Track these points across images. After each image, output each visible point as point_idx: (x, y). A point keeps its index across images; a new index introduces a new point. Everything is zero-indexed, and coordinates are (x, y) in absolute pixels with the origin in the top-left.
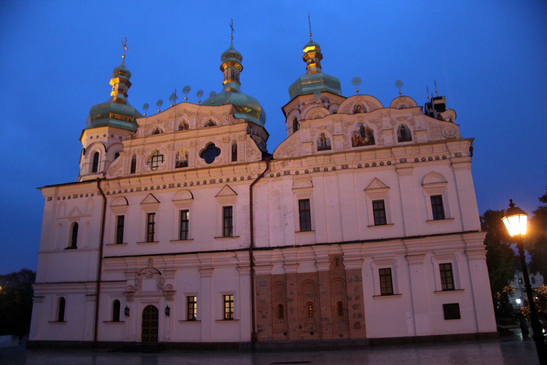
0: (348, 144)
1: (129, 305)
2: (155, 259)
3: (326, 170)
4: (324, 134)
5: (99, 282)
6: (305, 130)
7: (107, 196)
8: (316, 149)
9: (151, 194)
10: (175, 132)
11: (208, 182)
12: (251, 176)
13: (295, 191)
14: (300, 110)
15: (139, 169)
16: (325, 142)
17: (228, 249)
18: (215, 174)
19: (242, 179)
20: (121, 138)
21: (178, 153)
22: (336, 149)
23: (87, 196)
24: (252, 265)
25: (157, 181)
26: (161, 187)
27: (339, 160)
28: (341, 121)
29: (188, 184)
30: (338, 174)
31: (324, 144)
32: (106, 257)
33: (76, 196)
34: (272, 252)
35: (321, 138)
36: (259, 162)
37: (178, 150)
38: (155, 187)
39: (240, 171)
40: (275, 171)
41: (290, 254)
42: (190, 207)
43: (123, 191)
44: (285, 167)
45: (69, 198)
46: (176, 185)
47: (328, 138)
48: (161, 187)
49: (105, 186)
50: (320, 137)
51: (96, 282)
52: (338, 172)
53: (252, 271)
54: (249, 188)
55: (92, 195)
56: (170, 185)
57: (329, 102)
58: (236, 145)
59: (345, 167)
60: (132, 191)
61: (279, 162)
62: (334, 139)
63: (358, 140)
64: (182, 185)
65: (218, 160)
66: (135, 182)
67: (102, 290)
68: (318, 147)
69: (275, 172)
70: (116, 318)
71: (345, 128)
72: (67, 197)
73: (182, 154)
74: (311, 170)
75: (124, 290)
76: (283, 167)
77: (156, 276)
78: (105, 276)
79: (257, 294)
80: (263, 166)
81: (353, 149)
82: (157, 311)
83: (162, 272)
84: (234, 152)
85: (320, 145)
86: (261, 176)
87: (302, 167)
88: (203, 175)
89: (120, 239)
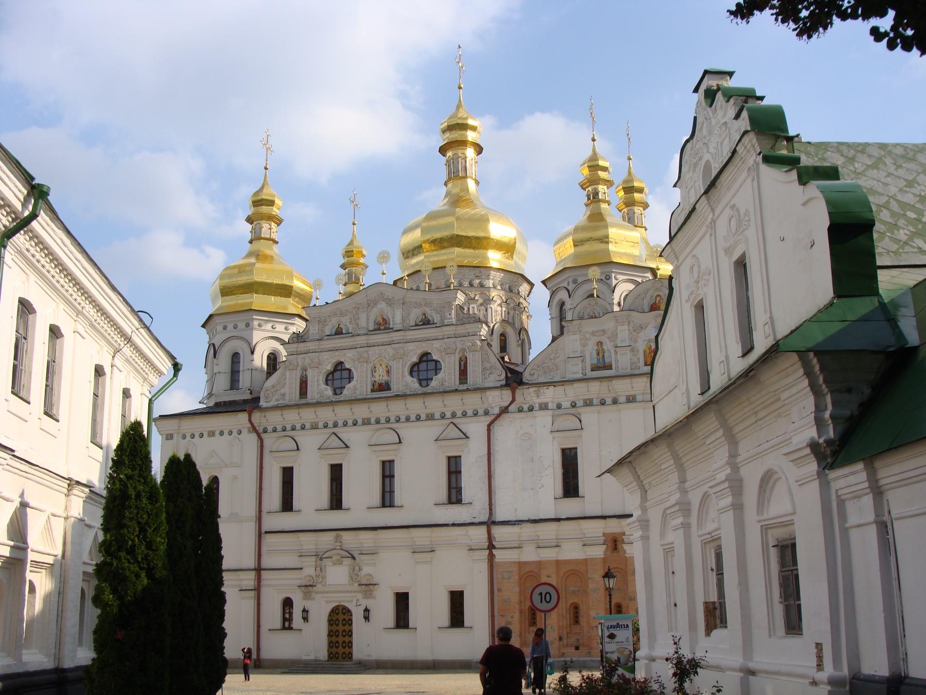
0: (638, 361)
1: (309, 605)
2: (346, 536)
3: (603, 403)
4: (601, 343)
5: (259, 570)
6: (572, 337)
7: (263, 436)
8: (589, 368)
9: (334, 433)
10: (369, 333)
12: (489, 409)
16: (604, 356)
17: (456, 522)
18: (435, 405)
19: (476, 414)
20: (274, 327)
21: (375, 367)
22: (620, 371)
23: (230, 433)
24: (491, 547)
25: (343, 413)
26: (350, 422)
27: (622, 388)
30: (620, 411)
31: (601, 360)
32: (266, 532)
33: (212, 434)
34: (521, 528)
35: (597, 350)
37: (375, 362)
38: (340, 423)
39: (472, 401)
41: (548, 532)
45: (201, 436)
46: (373, 421)
47: (608, 350)
50: (596, 348)
51: (255, 569)
52: (620, 406)
53: (491, 557)
54: (486, 428)
55: (240, 432)
56: (363, 420)
58: (466, 358)
59: (631, 400)
61: (532, 390)
62: (616, 353)
64: (383, 420)
65: (437, 382)
66: (308, 415)
67: (263, 583)
68: (591, 365)
70: (287, 624)
71: (634, 333)
72: (197, 435)
73: (381, 370)
74: (580, 403)
75: (298, 582)
76: (538, 396)
77: (348, 561)
78: (266, 562)
79: (499, 590)
80: (507, 394)
82: (349, 614)
83: (356, 556)
84: (462, 368)
85: (595, 361)
86: (505, 410)
88: (415, 406)
89: (287, 505)
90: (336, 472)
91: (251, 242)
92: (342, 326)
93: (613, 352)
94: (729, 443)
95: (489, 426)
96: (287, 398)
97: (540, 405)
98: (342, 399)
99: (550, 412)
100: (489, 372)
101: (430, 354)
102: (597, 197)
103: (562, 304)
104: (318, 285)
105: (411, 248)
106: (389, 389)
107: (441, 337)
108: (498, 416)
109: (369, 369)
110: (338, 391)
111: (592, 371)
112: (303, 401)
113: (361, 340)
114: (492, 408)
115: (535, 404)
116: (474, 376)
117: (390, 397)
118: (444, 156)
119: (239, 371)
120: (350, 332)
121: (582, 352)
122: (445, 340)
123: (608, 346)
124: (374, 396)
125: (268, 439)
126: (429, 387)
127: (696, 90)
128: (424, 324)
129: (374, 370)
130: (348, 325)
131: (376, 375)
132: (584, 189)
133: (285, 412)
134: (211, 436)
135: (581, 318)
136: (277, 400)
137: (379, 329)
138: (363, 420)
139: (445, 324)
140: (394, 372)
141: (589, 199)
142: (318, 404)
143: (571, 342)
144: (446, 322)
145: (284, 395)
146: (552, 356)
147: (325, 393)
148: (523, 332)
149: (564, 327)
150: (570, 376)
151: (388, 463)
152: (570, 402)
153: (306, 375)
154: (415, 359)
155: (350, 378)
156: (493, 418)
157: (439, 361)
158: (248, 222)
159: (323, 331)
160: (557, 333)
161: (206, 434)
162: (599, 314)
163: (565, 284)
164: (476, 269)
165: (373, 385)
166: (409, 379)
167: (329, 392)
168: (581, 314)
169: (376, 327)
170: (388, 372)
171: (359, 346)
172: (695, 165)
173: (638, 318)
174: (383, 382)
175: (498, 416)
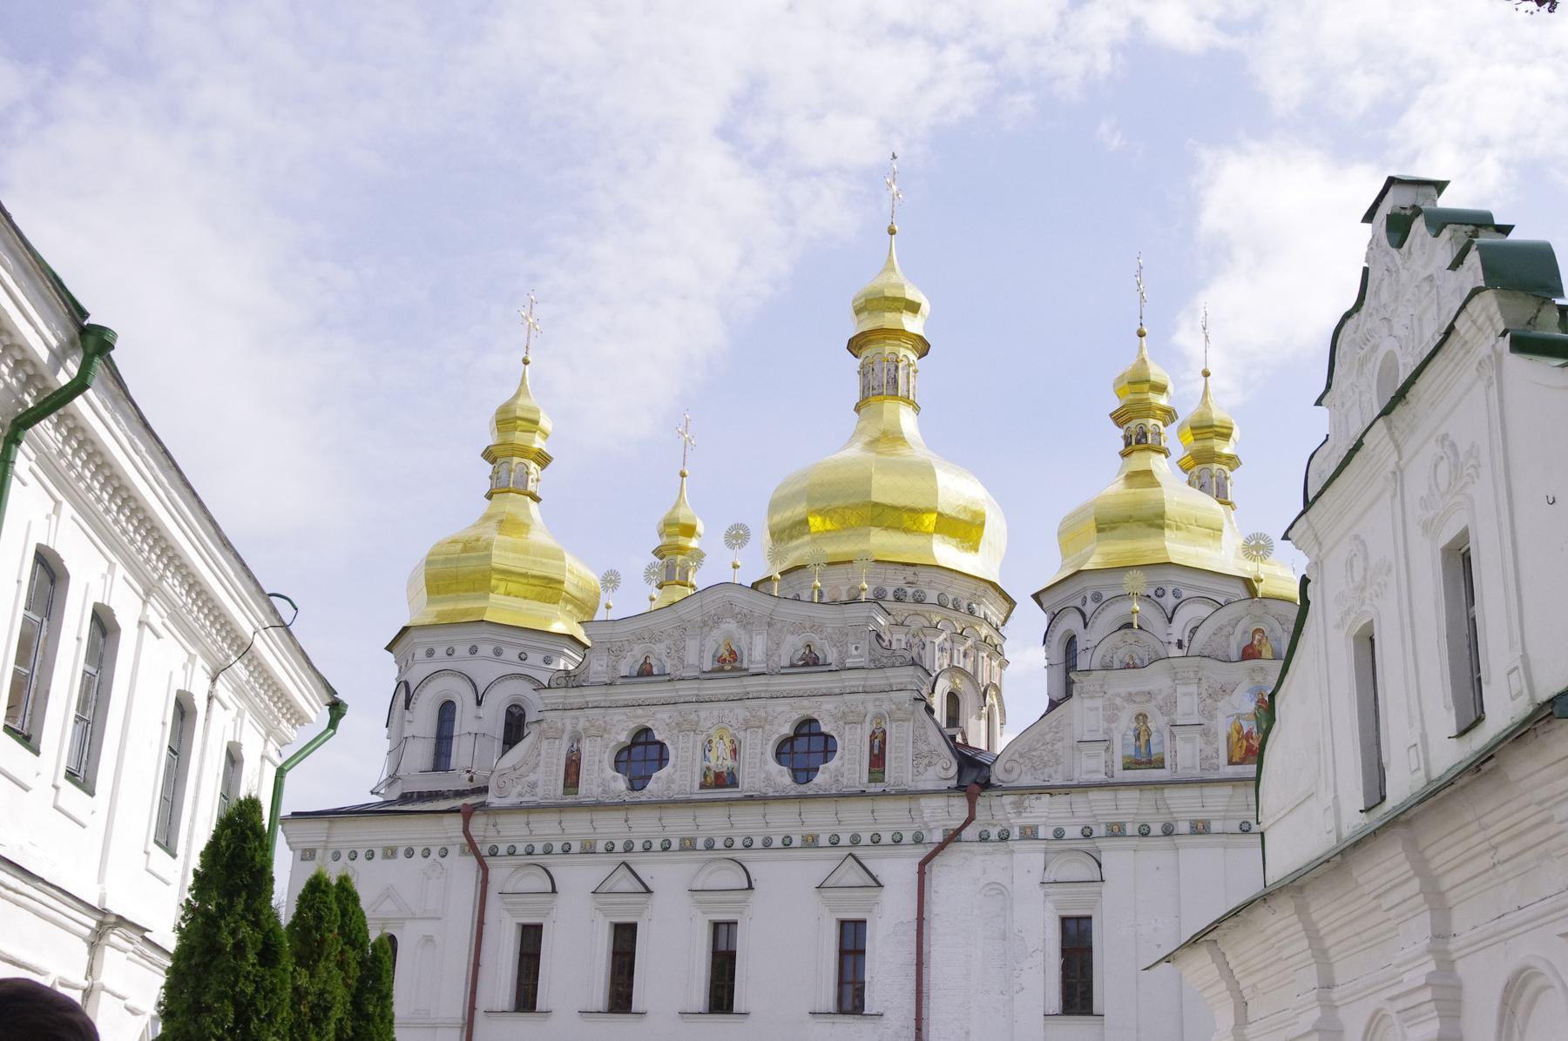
3: (1144, 833)
4: (1145, 716)
6: (1087, 703)
7: (489, 861)
8: (1118, 765)
9: (624, 863)
11: (797, 841)
13: (1050, 890)
14: (1083, 615)
15: (589, 786)
18: (820, 819)
19: (897, 841)
25: (645, 825)
27: (1184, 804)
28: (1200, 680)
29: (738, 843)
31: (1143, 750)
33: (390, 853)
35: (1136, 729)
36: (949, 791)
37: (711, 731)
39: (892, 816)
40: (995, 822)
42: (741, 913)
43: (539, 848)
44: (1024, 814)
46: (700, 844)
48: (657, 845)
49: (485, 831)
52: (1178, 840)
55: (444, 853)
56: (683, 840)
57: (1176, 594)
58: (884, 732)
59: (1200, 829)
60: (566, 850)
61: (1007, 799)
62: (1173, 736)
63: (1248, 741)
64: (719, 844)
65: (827, 776)
66: (577, 826)
69: (995, 825)
71: (1209, 701)
72: (361, 854)
73: (721, 747)
74: (1100, 830)
80: (959, 806)
81: (1231, 771)
84: (876, 752)
86: (953, 837)
87: (1073, 817)
88: (782, 820)
90: (625, 938)
91: (489, 496)
92: (652, 661)
93: (1167, 735)
94: (1432, 909)
95: (922, 864)
96: (540, 791)
97: (1023, 829)
98: (644, 799)
99: (1041, 845)
100: (926, 761)
101: (816, 721)
102: (1143, 440)
103: (1071, 643)
104: (611, 581)
105: (787, 524)
106: (734, 784)
107: (837, 691)
108: (941, 847)
109: (699, 745)
110: (637, 784)
111: (1124, 769)
112: (570, 799)
113: (687, 690)
114: (930, 830)
115: (1012, 826)
116: (899, 769)
117: (738, 800)
118: (856, 357)
119: (451, 737)
120: (667, 672)
121: (1108, 731)
122: (847, 697)
123: (1157, 723)
124: (705, 797)
125: (500, 873)
126: (811, 785)
127: (1369, 217)
128: (806, 665)
129: (708, 747)
130: (664, 658)
131: (712, 756)
132: (1120, 425)
133: (533, 818)
134: (389, 858)
135: (1107, 668)
136: (520, 795)
137: (722, 670)
138: (683, 840)
139: (847, 665)
140: (745, 753)
141: (1128, 444)
142: (597, 806)
143: (1084, 714)
144: (849, 663)
145: (533, 785)
146: (1048, 737)
147: (613, 785)
148: (992, 693)
149: (1073, 682)
150: (1081, 777)
151: (725, 927)
152: (1080, 828)
153: (578, 750)
154: (787, 730)
155: (662, 760)
156: (930, 849)
157: (833, 737)
158: (486, 458)
159: (615, 668)
160: (1059, 693)
161: (378, 853)
162: (1142, 660)
163: (1078, 603)
164: (908, 568)
165: (705, 776)
166: (773, 766)
167: (620, 784)
168: (1108, 659)
169: (717, 665)
170: (734, 751)
171: (682, 700)
172: (1363, 363)
173: (1218, 673)
174: (725, 770)
175: (941, 847)
